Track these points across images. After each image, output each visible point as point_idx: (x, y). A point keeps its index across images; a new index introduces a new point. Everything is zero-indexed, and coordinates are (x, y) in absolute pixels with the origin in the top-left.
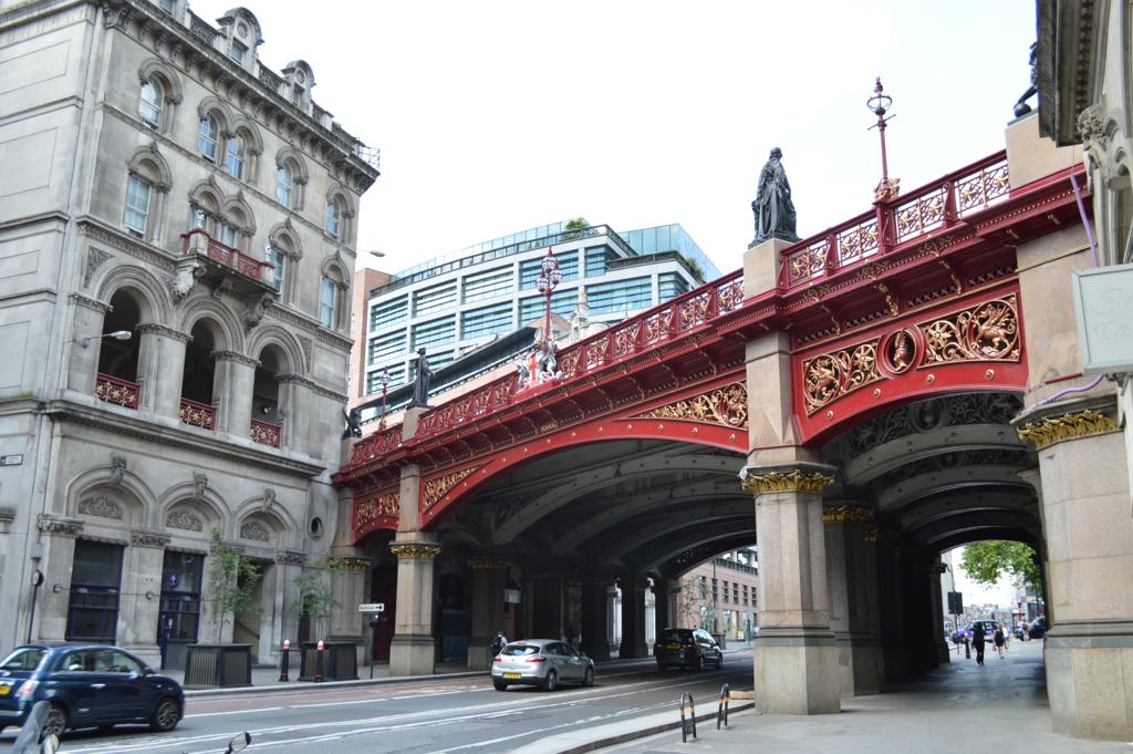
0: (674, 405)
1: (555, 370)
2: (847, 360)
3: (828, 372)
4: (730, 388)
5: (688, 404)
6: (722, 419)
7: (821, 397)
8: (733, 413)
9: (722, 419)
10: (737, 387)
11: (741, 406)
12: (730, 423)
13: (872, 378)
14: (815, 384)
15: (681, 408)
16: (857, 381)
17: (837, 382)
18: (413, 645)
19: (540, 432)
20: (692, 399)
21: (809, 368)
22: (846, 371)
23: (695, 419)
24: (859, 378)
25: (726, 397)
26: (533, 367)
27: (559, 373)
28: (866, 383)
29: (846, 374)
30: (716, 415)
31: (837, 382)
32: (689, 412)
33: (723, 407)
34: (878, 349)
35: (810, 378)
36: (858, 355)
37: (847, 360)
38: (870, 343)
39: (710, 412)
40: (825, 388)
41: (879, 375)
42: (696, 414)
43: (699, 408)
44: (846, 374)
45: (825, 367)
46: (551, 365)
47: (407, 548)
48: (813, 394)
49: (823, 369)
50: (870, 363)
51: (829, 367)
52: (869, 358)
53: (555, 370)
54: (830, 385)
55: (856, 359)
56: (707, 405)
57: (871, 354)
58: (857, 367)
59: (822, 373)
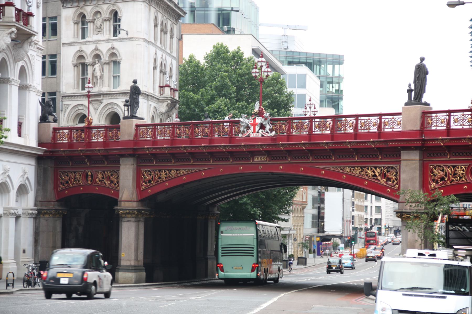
0: (354, 167)
1: (271, 130)
2: (451, 169)
3: (442, 173)
4: (389, 167)
5: (361, 168)
6: (383, 181)
7: (437, 182)
8: (389, 179)
9: (383, 181)
10: (392, 168)
11: (394, 177)
12: (387, 184)
13: (463, 181)
14: (435, 176)
15: (357, 171)
16: (456, 180)
17: (446, 179)
18: (135, 272)
19: (253, 161)
20: (365, 167)
21: (432, 169)
22: (451, 174)
23: (366, 178)
24: (457, 179)
25: (385, 171)
26: (254, 125)
27: (274, 133)
28: (460, 182)
29: (450, 176)
30: (379, 178)
31: (446, 179)
32: (363, 173)
33: (384, 176)
34: (467, 169)
35: (432, 173)
36: (457, 169)
37: (451, 169)
38: (463, 165)
39: (375, 175)
40: (439, 179)
41: (466, 180)
42: (367, 175)
43: (370, 172)
44: (450, 176)
45: (441, 170)
46: (268, 127)
47: (130, 212)
48: (433, 181)
49: (440, 171)
50: (462, 174)
51: (443, 171)
52: (462, 172)
53: (271, 130)
54: (442, 179)
55: (456, 170)
56: (374, 172)
57: (463, 171)
58: (456, 174)
59: (439, 173)
